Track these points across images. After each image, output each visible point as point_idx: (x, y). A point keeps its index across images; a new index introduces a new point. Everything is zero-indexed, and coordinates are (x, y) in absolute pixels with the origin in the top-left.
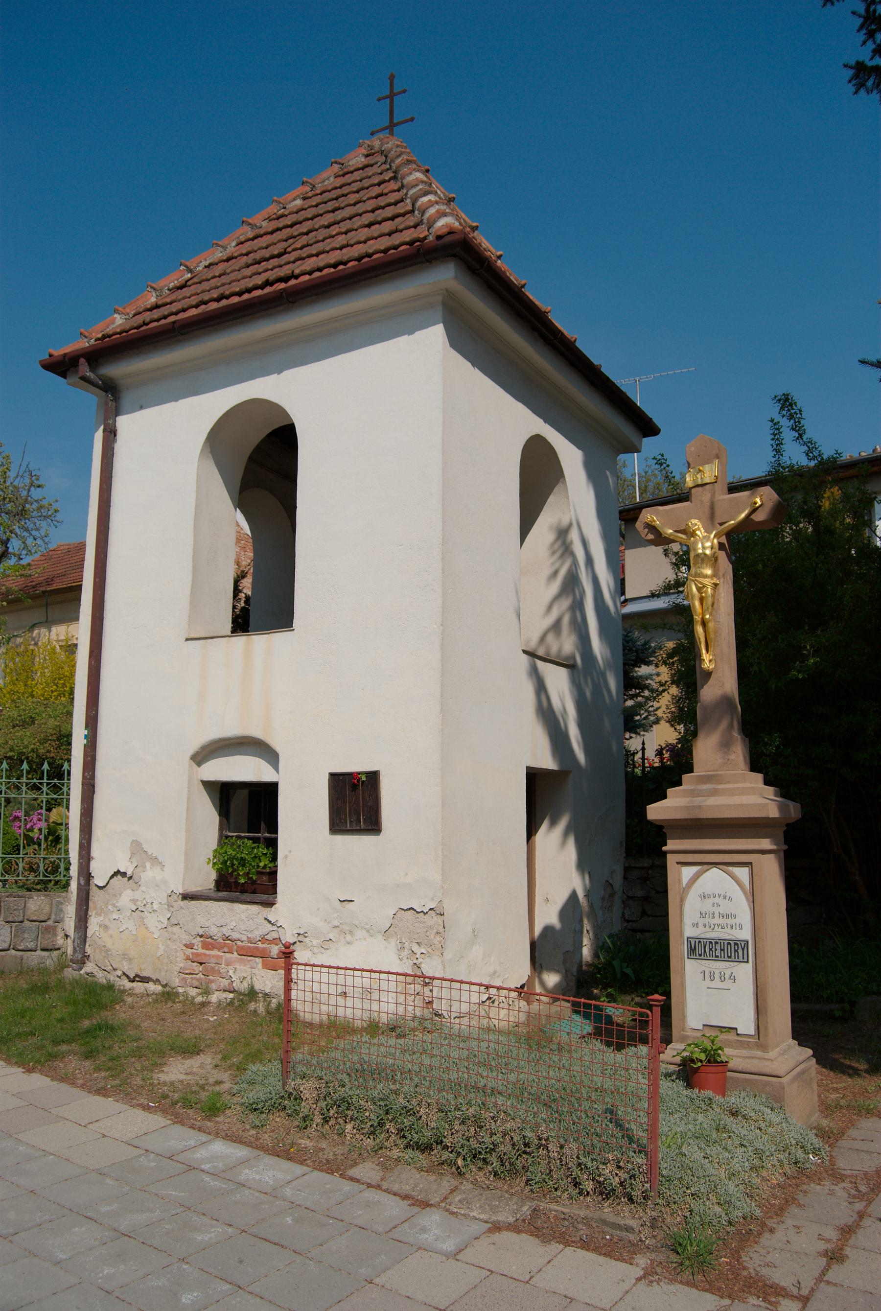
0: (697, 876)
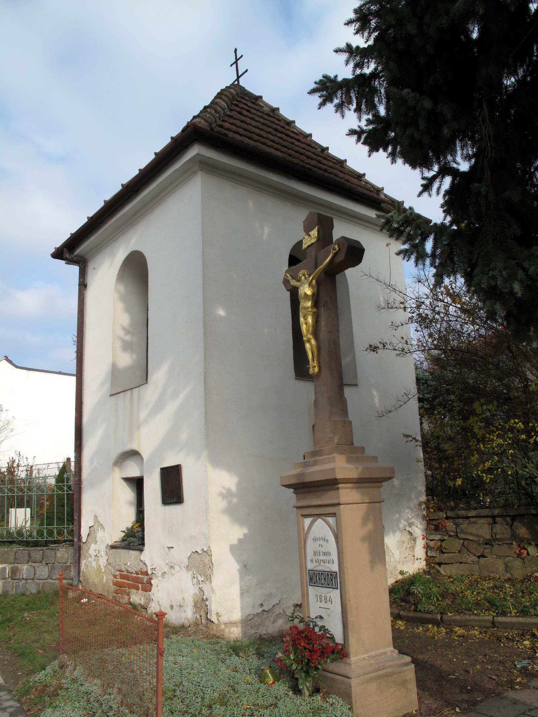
0: (312, 523)
